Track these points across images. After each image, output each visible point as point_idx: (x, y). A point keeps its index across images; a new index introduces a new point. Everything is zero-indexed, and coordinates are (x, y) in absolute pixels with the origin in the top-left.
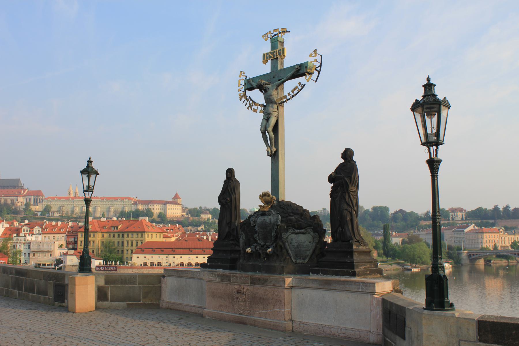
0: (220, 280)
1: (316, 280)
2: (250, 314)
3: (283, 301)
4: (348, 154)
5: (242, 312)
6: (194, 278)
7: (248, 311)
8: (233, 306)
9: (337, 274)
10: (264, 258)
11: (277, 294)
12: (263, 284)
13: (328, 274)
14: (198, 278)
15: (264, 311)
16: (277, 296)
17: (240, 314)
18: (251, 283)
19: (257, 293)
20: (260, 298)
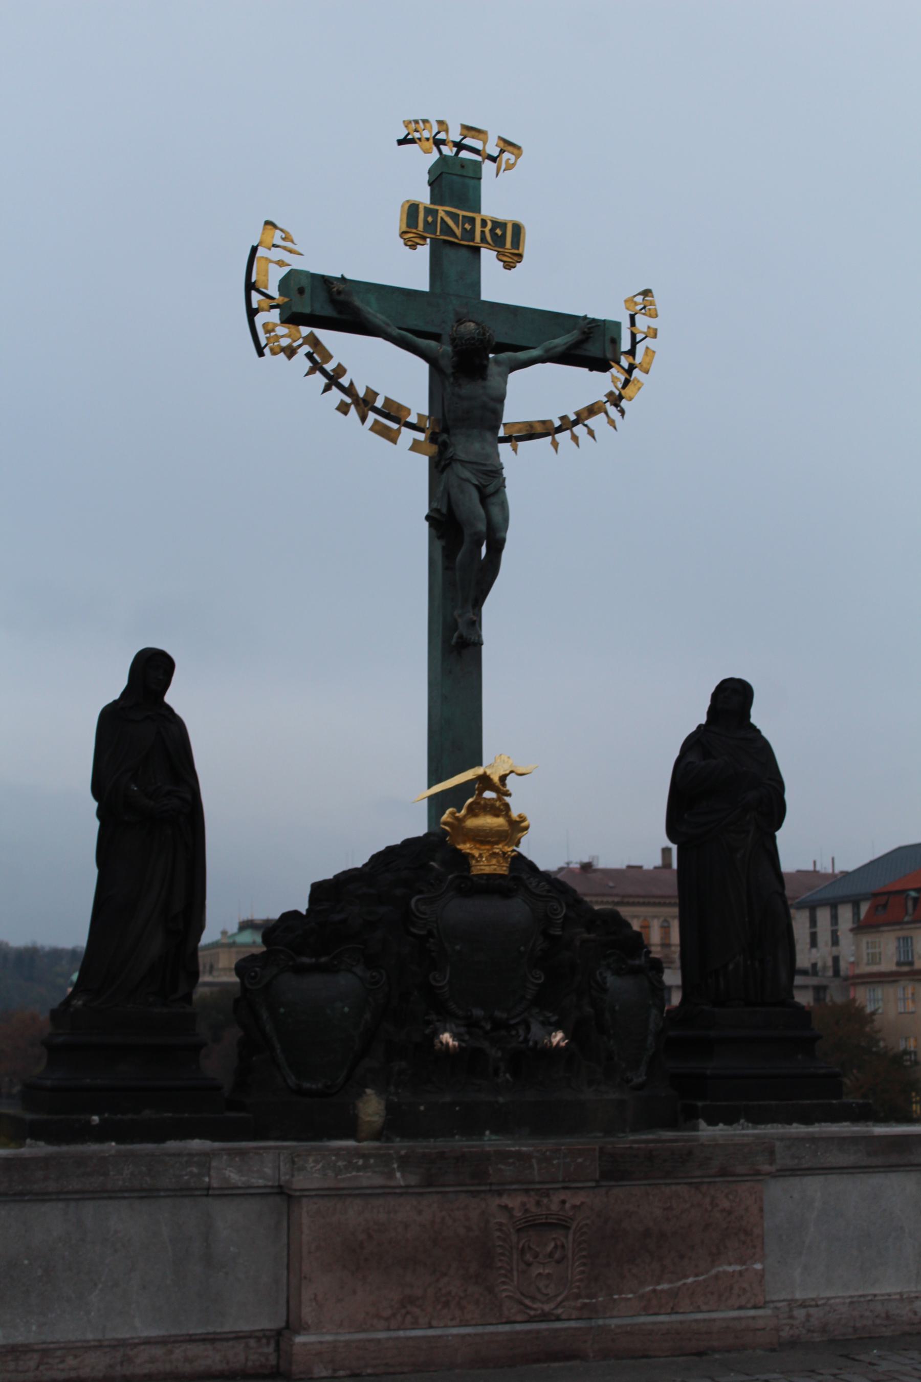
0: (413, 1180)
1: (854, 1140)
4: (732, 699)
5: (547, 1308)
6: (148, 1194)
7: (578, 1296)
10: (496, 1072)
14: (185, 1192)
15: (664, 1286)
16: (730, 1213)
17: (545, 1317)
18: (607, 1175)
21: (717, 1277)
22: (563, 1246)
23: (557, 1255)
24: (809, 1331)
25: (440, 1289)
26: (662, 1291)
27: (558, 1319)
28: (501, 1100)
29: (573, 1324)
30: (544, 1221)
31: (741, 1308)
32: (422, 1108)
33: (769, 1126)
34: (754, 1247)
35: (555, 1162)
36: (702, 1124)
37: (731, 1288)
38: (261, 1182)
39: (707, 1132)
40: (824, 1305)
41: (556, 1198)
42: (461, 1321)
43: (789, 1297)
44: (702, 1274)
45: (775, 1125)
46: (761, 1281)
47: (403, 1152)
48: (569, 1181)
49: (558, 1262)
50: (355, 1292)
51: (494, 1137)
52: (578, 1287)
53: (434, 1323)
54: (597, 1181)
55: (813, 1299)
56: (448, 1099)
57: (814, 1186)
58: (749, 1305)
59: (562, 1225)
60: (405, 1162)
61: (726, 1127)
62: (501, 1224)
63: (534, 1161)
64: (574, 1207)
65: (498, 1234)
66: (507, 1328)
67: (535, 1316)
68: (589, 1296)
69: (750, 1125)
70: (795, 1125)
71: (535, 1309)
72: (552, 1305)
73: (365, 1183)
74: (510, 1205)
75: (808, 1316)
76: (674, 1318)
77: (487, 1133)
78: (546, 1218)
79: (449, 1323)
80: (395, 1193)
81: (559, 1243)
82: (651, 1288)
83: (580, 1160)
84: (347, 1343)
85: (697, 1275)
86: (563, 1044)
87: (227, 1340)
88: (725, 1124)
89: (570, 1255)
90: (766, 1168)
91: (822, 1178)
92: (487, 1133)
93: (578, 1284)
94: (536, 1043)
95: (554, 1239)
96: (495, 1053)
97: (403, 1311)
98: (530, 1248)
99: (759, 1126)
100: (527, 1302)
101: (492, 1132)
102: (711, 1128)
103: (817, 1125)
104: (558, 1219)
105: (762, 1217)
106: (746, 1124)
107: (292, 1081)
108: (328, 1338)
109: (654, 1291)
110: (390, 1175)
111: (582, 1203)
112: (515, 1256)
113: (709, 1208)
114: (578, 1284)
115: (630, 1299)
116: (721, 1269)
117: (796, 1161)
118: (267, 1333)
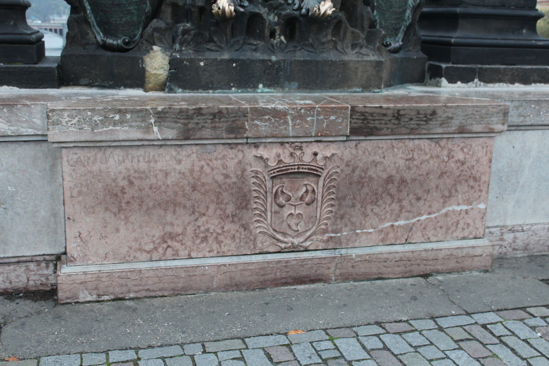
2: (334, 243)
3: (484, 178)
5: (296, 241)
7: (325, 231)
8: (245, 227)
9: (526, 80)
10: (272, 35)
11: (461, 156)
12: (412, 131)
13: (500, 81)
15: (401, 223)
16: (463, 163)
17: (294, 249)
18: (355, 131)
19: (375, 164)
20: (390, 180)
21: (446, 215)
22: (313, 191)
23: (307, 199)
24: (514, 249)
25: (199, 227)
26: (399, 226)
27: (306, 250)
28: (274, 58)
29: (319, 254)
30: (296, 170)
31: (464, 238)
32: (202, 64)
33: (497, 85)
34: (481, 191)
35: (308, 119)
36: (444, 81)
37: (458, 223)
38: (31, 131)
39: (447, 89)
40: (529, 230)
41: (309, 151)
42: (218, 252)
43: (502, 224)
44: (434, 213)
45: (501, 84)
46: (483, 218)
47: (160, 109)
48: (321, 136)
49: (308, 204)
50: (118, 230)
51: (266, 90)
52: (326, 224)
53: (193, 255)
54: (347, 136)
55: (520, 226)
56: (226, 56)
57: (532, 137)
58: (471, 236)
59: (314, 173)
60: (162, 117)
61: (463, 85)
62: (257, 172)
63: (289, 117)
64: (326, 158)
65: (255, 180)
66: (260, 258)
67: (285, 248)
68: (333, 232)
69: (482, 83)
70: (516, 84)
71: (286, 243)
72: (301, 239)
73: (122, 136)
74: (265, 156)
75: (515, 238)
76: (408, 248)
77: (261, 86)
78: (298, 168)
79: (207, 254)
80: (154, 145)
81: (309, 188)
82: (390, 224)
83: (333, 118)
84: (110, 274)
85: (430, 214)
86: (330, 12)
87: (9, 264)
88: (462, 82)
89: (320, 199)
90: (499, 127)
91: (540, 132)
92: (261, 86)
93: (326, 221)
94: (308, 10)
95: (306, 185)
96: (273, 18)
97: (165, 246)
98: (282, 192)
99: (489, 85)
100: (279, 236)
101: (264, 86)
102: (451, 85)
103: (533, 85)
104: (309, 169)
105: (490, 167)
106: (479, 82)
107: (100, 37)
108: (93, 269)
109: (392, 226)
110: (148, 129)
111: (333, 155)
112: (269, 200)
113: (446, 159)
114: (326, 221)
115: (370, 233)
116: (450, 209)
117: (522, 118)
118: (47, 258)
